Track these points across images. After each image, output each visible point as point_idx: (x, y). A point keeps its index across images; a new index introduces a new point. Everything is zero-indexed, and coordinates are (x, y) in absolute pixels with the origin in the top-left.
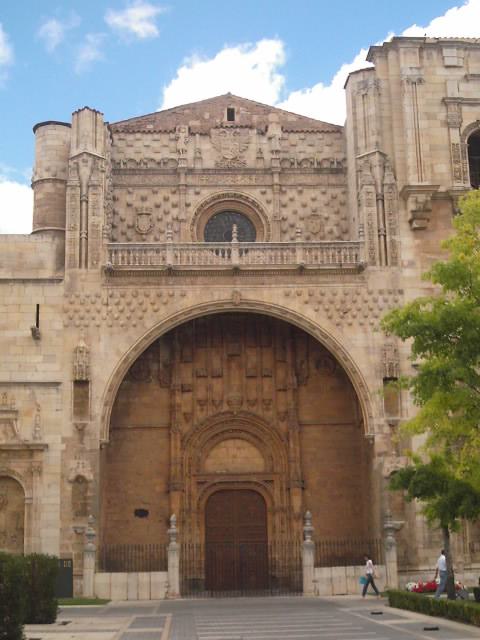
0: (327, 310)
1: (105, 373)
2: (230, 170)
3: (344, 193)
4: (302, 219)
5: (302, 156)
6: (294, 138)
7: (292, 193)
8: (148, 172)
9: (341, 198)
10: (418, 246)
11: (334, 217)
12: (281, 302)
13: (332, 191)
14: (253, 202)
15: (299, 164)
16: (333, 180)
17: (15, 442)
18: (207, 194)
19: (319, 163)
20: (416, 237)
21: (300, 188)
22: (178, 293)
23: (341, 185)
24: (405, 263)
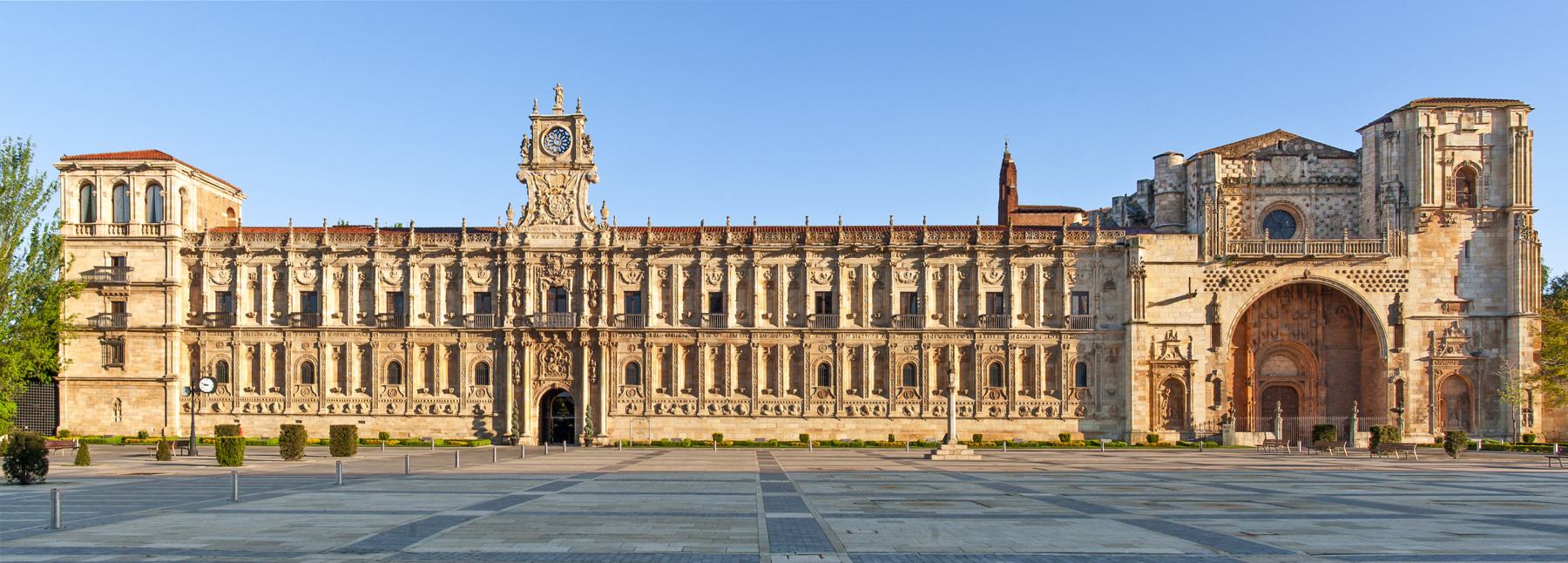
0: (1361, 281)
1: (1228, 317)
2: (1283, 184)
3: (1356, 200)
4: (1328, 217)
5: (1329, 175)
6: (1325, 161)
7: (1322, 200)
8: (1231, 185)
9: (1354, 203)
10: (1420, 243)
11: (1348, 216)
12: (1334, 277)
13: (1349, 198)
14: (1297, 206)
15: (1328, 180)
16: (1349, 191)
17: (1179, 359)
18: (1268, 201)
19: (1341, 180)
20: (1419, 237)
21: (1328, 196)
22: (1271, 271)
23: (1353, 194)
24: (1412, 254)
